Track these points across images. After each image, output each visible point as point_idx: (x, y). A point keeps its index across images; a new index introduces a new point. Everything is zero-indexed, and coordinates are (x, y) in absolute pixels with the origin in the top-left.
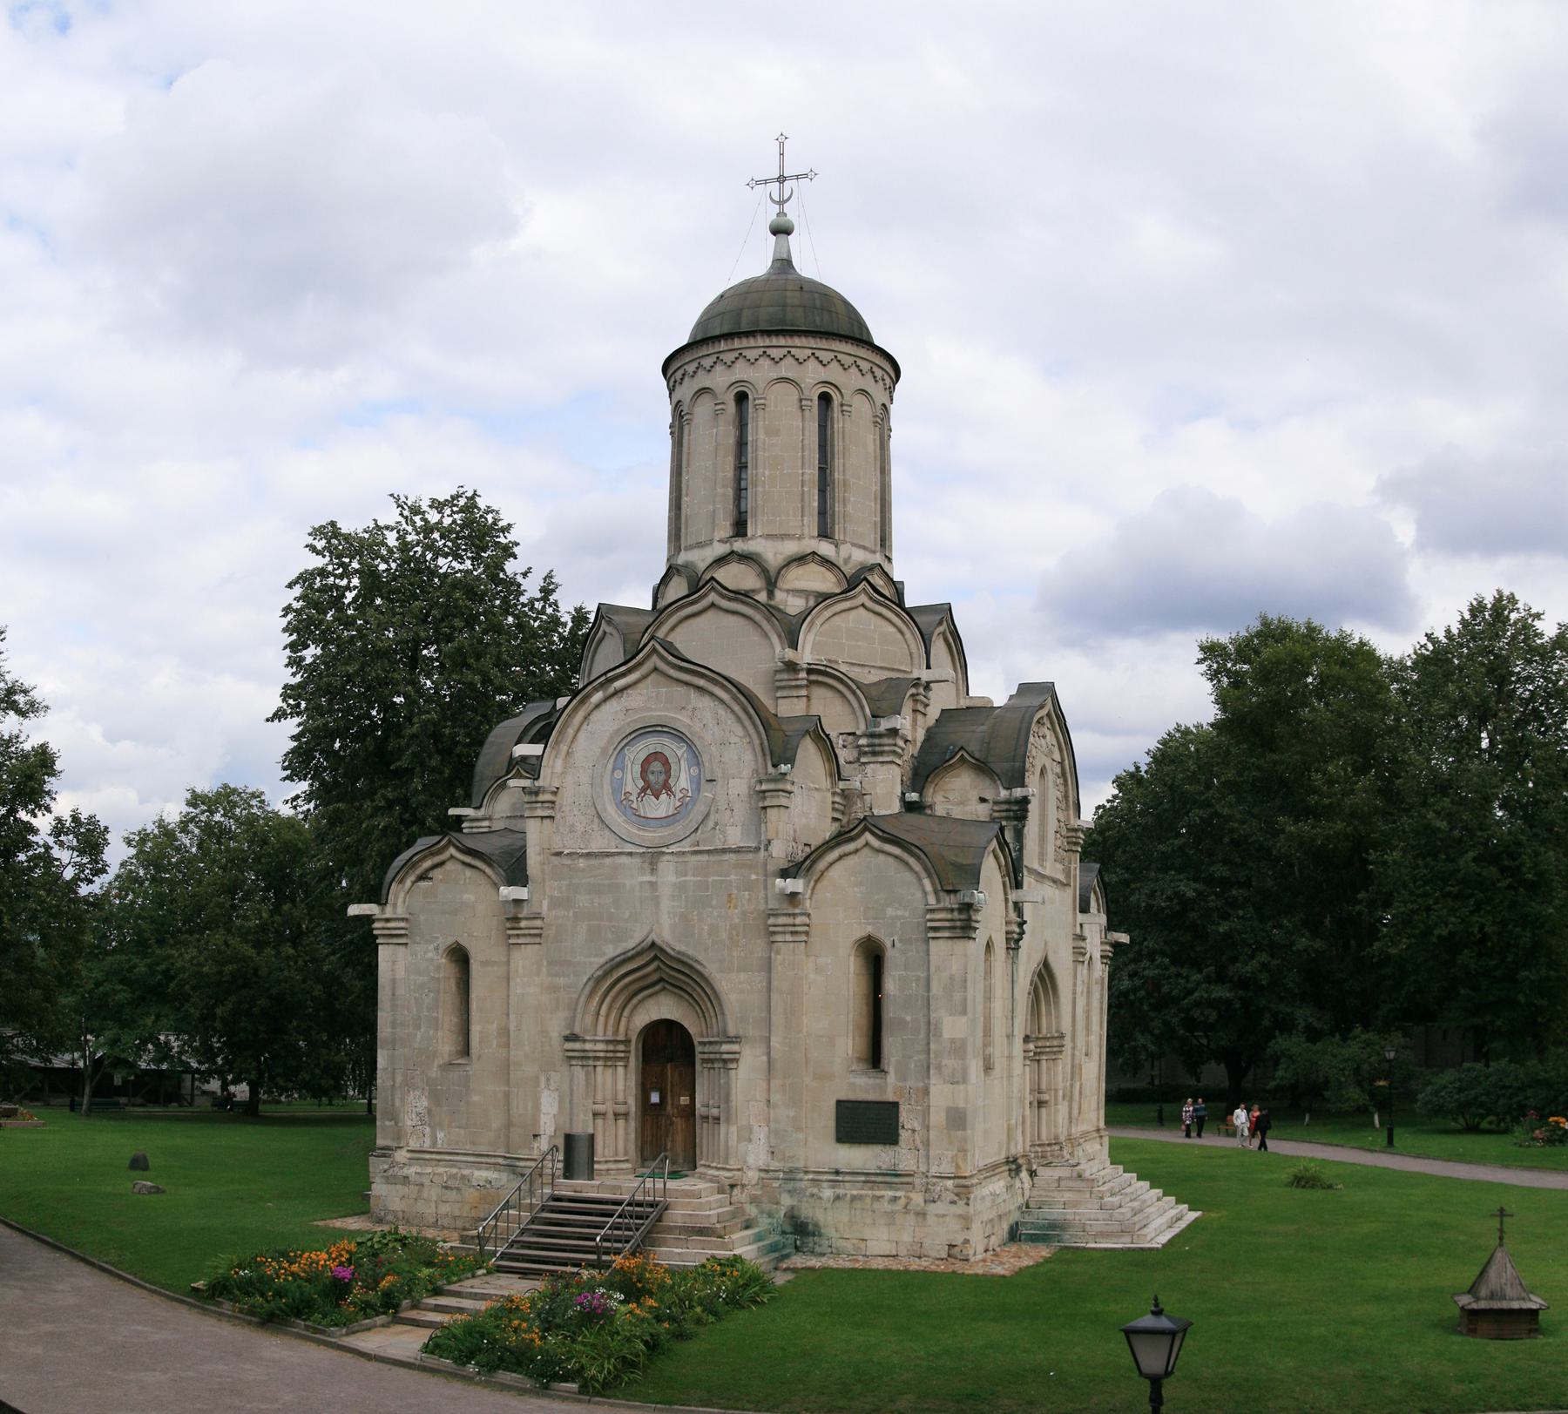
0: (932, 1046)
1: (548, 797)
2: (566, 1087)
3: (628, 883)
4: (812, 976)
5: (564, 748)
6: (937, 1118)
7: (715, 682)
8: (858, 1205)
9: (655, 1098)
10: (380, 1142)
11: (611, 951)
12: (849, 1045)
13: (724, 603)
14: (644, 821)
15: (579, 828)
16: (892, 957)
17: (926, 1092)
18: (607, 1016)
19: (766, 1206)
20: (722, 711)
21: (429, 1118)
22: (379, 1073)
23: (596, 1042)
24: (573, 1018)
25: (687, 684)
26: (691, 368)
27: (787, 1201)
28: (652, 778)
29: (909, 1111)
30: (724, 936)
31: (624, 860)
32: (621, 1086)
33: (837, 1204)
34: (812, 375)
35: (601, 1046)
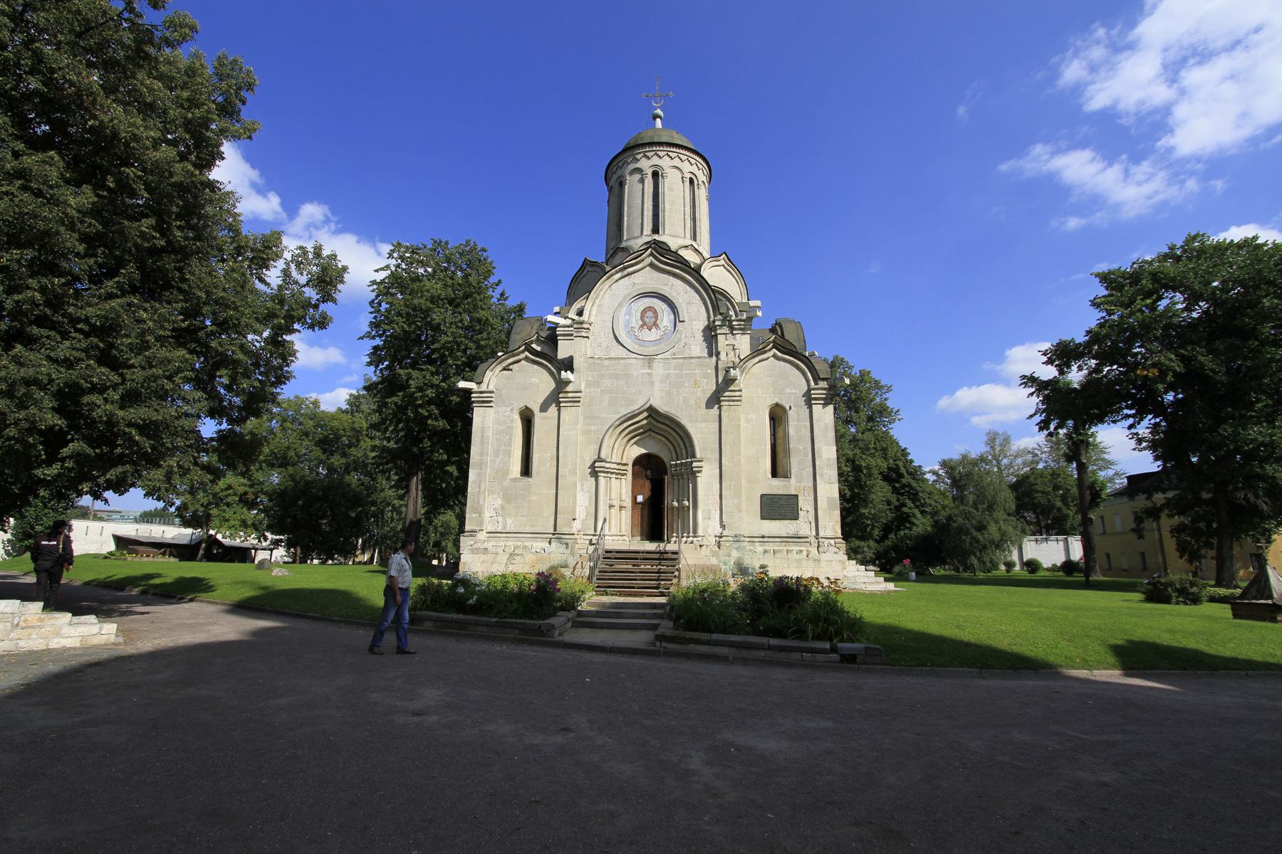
5: (597, 302)
8: (778, 555)
10: (467, 527)
15: (605, 345)
19: (722, 558)
21: (502, 512)
27: (735, 554)
30: (692, 402)
34: (686, 167)
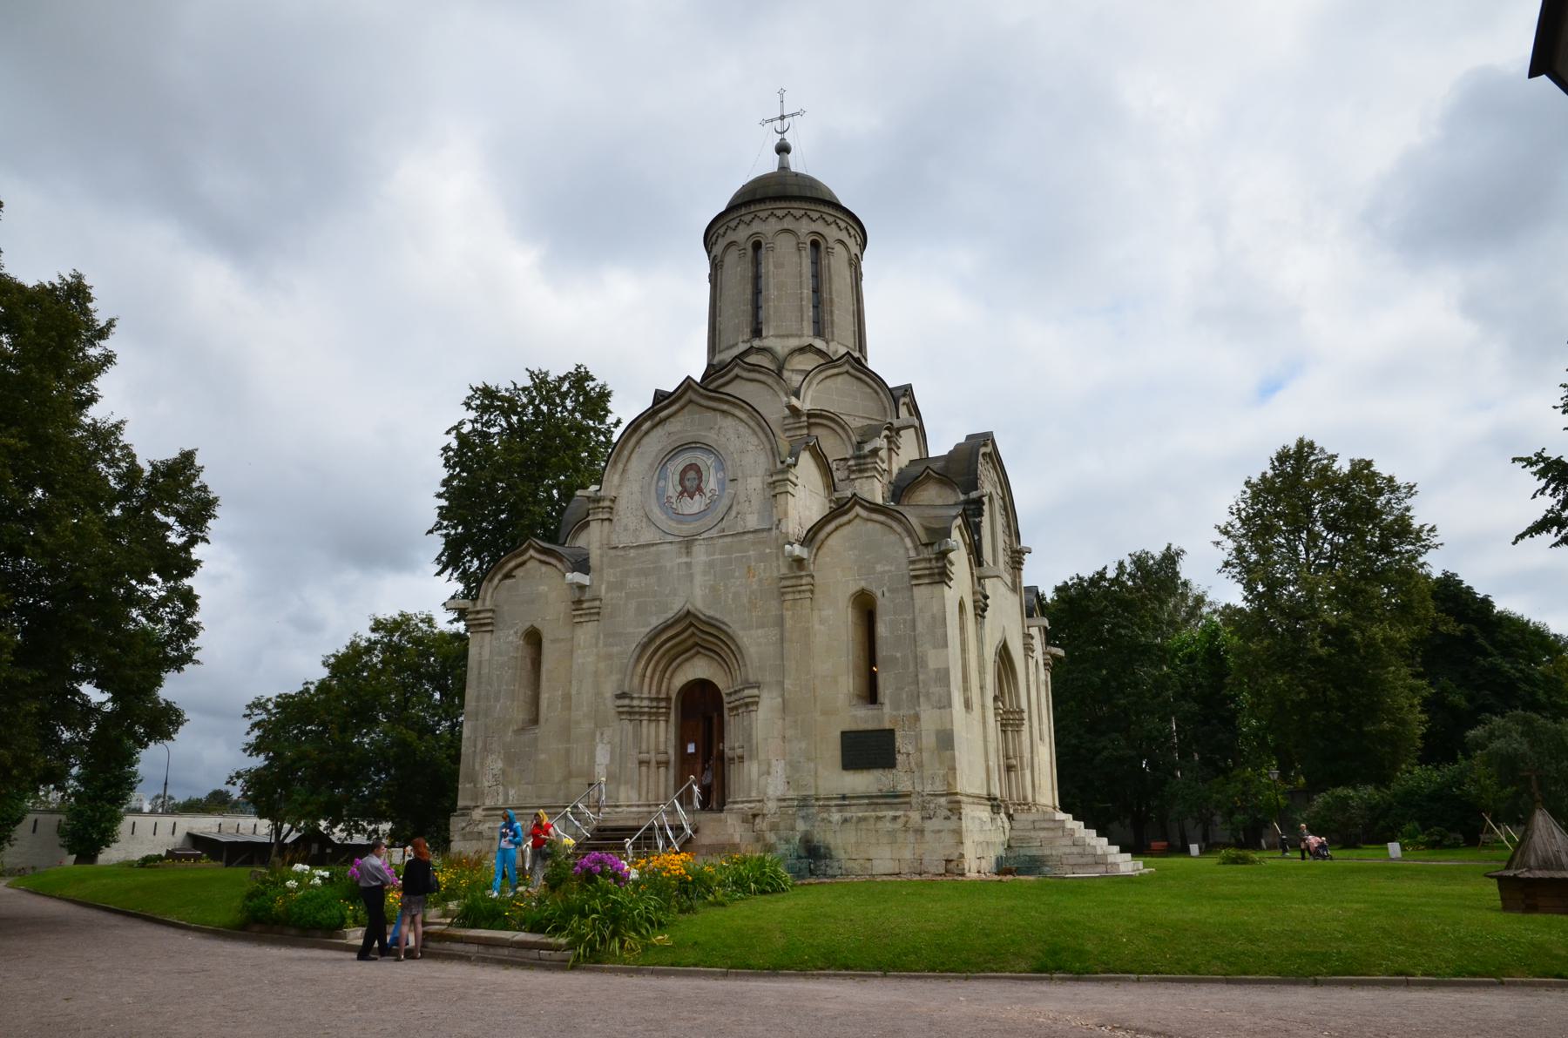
0: (921, 677)
1: (607, 503)
2: (617, 740)
3: (669, 565)
4: (817, 626)
5: (620, 466)
6: (929, 740)
7: (734, 404)
8: (863, 825)
9: (691, 748)
10: (461, 803)
11: (655, 621)
12: (847, 683)
13: (745, 374)
15: (632, 527)
16: (883, 605)
17: (917, 718)
18: (652, 678)
19: (783, 833)
20: (742, 428)
21: (503, 779)
22: (464, 742)
23: (641, 699)
24: (623, 680)
25: (715, 410)
26: (721, 231)
27: (801, 826)
28: (687, 484)
29: (904, 737)
30: (745, 600)
31: (667, 547)
32: (662, 739)
33: (848, 825)
34: (805, 227)
35: (646, 703)
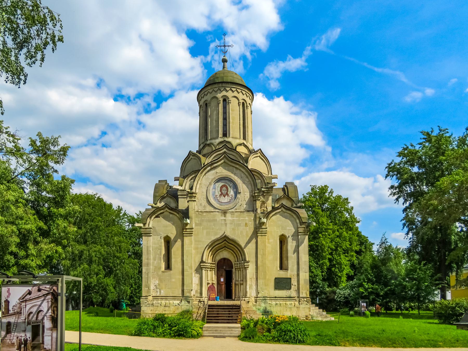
14: (221, 203)
15: (203, 204)
26: (211, 91)
31: (217, 213)
34: (241, 96)
